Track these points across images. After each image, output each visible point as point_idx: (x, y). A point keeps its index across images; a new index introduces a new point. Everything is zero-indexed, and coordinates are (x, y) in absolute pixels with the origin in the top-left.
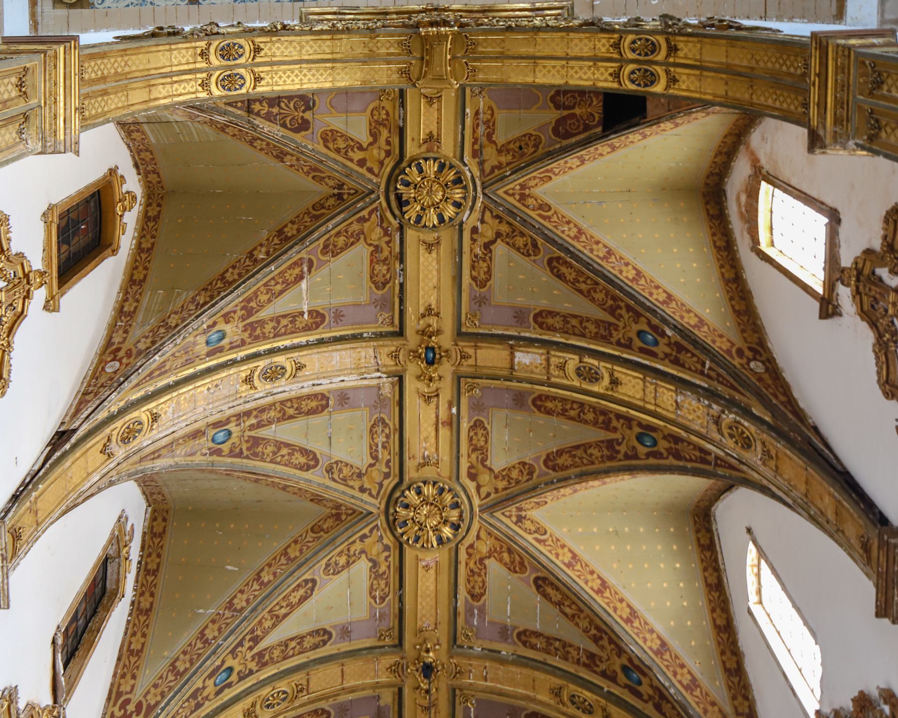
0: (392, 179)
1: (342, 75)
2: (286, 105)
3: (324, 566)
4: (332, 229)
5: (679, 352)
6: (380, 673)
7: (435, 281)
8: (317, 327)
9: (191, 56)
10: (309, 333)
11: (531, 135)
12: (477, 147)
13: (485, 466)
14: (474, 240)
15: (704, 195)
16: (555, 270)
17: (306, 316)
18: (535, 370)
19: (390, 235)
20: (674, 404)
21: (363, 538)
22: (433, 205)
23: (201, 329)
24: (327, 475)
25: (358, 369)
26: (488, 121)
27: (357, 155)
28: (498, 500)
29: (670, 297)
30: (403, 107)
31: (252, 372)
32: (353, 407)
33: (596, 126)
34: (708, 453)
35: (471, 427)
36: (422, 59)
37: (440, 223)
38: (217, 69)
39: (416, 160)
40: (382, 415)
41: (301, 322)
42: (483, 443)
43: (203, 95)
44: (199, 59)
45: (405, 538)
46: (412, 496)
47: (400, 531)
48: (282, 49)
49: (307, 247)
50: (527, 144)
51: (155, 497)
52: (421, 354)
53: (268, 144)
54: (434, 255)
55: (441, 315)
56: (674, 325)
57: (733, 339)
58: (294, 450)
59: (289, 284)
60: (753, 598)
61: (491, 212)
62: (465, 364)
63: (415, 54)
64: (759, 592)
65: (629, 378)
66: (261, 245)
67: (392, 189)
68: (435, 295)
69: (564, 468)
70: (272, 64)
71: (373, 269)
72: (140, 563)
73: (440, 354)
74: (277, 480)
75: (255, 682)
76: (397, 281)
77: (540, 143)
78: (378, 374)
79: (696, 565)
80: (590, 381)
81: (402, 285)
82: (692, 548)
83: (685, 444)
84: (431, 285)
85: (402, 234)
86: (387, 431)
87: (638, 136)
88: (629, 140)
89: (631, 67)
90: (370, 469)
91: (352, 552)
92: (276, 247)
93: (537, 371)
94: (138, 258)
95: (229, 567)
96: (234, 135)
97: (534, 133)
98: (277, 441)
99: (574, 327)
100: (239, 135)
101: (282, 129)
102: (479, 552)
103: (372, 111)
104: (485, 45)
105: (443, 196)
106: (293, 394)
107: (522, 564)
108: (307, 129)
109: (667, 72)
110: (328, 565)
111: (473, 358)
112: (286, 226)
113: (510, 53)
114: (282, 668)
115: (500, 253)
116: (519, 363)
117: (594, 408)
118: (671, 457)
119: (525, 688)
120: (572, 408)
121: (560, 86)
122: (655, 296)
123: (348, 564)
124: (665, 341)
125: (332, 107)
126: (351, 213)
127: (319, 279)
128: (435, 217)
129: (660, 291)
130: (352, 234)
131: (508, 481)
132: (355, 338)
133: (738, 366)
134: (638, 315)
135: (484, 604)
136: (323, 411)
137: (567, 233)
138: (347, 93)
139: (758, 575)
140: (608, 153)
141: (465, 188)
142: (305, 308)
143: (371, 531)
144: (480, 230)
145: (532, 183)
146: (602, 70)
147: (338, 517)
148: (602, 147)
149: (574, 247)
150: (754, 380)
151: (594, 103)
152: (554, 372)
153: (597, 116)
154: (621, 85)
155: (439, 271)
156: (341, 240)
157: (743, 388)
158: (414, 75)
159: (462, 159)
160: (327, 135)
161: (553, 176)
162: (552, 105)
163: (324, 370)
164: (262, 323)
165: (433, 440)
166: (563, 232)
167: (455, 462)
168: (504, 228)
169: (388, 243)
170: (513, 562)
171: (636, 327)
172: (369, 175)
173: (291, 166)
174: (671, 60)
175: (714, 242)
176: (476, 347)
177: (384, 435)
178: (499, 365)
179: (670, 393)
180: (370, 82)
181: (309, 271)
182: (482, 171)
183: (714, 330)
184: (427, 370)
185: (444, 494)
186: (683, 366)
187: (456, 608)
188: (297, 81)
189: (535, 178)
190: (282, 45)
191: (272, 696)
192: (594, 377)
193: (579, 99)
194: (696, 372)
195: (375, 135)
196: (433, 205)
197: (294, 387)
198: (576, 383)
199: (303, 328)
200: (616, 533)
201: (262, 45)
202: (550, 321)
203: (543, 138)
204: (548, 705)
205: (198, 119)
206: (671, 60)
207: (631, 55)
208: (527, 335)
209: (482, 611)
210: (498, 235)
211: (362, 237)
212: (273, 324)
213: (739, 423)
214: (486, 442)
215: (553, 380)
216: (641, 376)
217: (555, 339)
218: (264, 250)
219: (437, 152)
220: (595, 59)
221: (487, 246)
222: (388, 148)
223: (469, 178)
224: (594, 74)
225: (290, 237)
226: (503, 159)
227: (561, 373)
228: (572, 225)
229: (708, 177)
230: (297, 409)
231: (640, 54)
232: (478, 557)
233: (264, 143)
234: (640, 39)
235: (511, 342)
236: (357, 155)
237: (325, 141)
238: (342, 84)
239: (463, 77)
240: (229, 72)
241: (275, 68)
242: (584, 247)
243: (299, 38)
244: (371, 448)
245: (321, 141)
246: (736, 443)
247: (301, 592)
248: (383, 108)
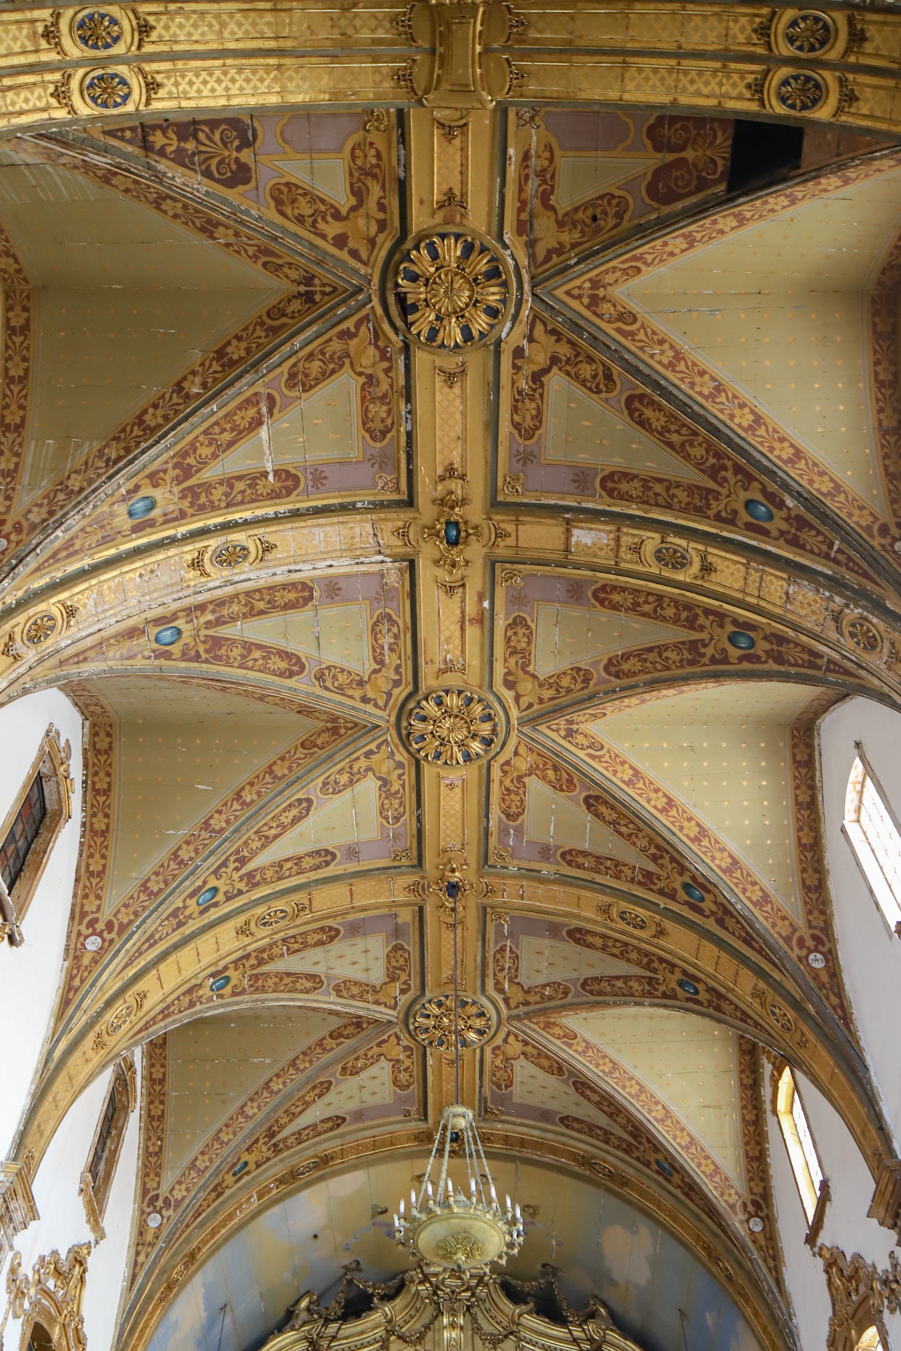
0: (389, 269)
1: (297, 81)
3: (320, 785)
4: (301, 349)
5: (799, 529)
6: (396, 893)
7: (458, 429)
8: (289, 493)
9: (27, 37)
10: (277, 501)
11: (613, 196)
12: (524, 216)
13: (527, 673)
14: (517, 368)
15: (874, 302)
16: (637, 414)
17: (271, 477)
18: (599, 553)
19: (390, 360)
20: (784, 596)
21: (368, 755)
22: (455, 312)
23: (117, 496)
24: (317, 683)
25: (350, 550)
26: (544, 170)
27: (333, 229)
28: (544, 711)
29: (798, 454)
30: (404, 143)
31: (201, 553)
32: (347, 600)
33: (717, 182)
34: (820, 656)
35: (509, 625)
36: (433, 51)
37: (465, 342)
38: (78, 64)
39: (428, 236)
40: (388, 610)
41: (264, 487)
42: (524, 645)
43: (61, 114)
44: (43, 44)
45: (423, 754)
46: (430, 708)
47: (416, 747)
48: (188, 28)
49: (263, 376)
50: (605, 213)
51: (91, 708)
52: (439, 531)
53: (185, 207)
54: (457, 389)
55: (468, 478)
56: (798, 493)
57: (878, 512)
58: (270, 653)
59: (240, 432)
60: (849, 815)
61: (545, 325)
62: (502, 544)
63: (420, 42)
64: (858, 810)
65: (727, 563)
66: (193, 373)
67: (390, 285)
68: (459, 449)
69: (631, 674)
70: (173, 57)
71: (367, 410)
72: (85, 782)
73: (466, 531)
74: (250, 689)
75: (246, 901)
76: (402, 429)
77: (625, 212)
78: (380, 558)
79: (787, 783)
80: (674, 567)
81: (409, 435)
82: (785, 766)
83: (792, 645)
84: (453, 434)
85: (407, 358)
86: (395, 630)
87: (783, 201)
88: (768, 207)
89: (784, 72)
90: (373, 676)
91: (355, 770)
92: (217, 375)
93: (602, 554)
94: (8, 392)
95: (200, 787)
96: (127, 191)
97: (618, 193)
98: (246, 642)
99: (657, 494)
100: (135, 191)
101: (206, 181)
102: (517, 769)
103: (353, 149)
104: (540, 26)
105: (470, 298)
106: (262, 583)
107: (570, 782)
108: (247, 181)
109: (842, 82)
110: (325, 784)
111: (513, 537)
112: (228, 343)
113: (582, 43)
114: (277, 889)
115: (556, 387)
116: (578, 543)
117: (676, 602)
118: (770, 661)
119: (569, 905)
120: (646, 602)
121: (663, 107)
122: (777, 453)
123: (351, 783)
124: (783, 514)
125: (285, 141)
126: (329, 324)
127: (286, 425)
128: (458, 331)
129: (786, 444)
130: (331, 357)
131: (557, 690)
132: (345, 508)
133: (878, 548)
134: (750, 478)
135: (522, 824)
136: (305, 605)
137: (657, 358)
138: (308, 116)
139: (861, 793)
140: (733, 229)
141: (505, 284)
142: (269, 467)
143: (379, 747)
144: (527, 353)
145: (609, 278)
146: (736, 77)
147: (335, 731)
148: (724, 220)
149: (666, 379)
150: (896, 566)
151: (718, 141)
152: (624, 554)
153: (720, 164)
154: (764, 106)
155: (464, 414)
156: (315, 367)
157: (879, 575)
158: (420, 84)
159: (500, 237)
160: (281, 192)
161: (643, 268)
162: (649, 143)
163: (303, 551)
165: (458, 642)
166: (652, 356)
167: (487, 667)
168: (564, 350)
169: (387, 371)
170: (559, 780)
171: (744, 496)
172: (353, 263)
173: (228, 245)
174: (852, 59)
175: (876, 374)
176: (518, 522)
177: (391, 634)
178: (550, 546)
179: (780, 583)
180: (346, 95)
181: (271, 412)
182: (532, 257)
183: (854, 499)
184: (448, 551)
185: (472, 705)
186: (803, 547)
187: (487, 828)
188: (220, 90)
189: (614, 269)
190: (187, 18)
191: (269, 914)
192: (679, 561)
193: (693, 133)
194: (818, 555)
195: (359, 194)
196: (455, 312)
197: (262, 573)
198: (655, 570)
199: (268, 494)
200: (692, 748)
201: (151, 20)
202: (624, 487)
203: (630, 199)
204: (594, 922)
205: (63, 160)
206: (852, 59)
207: (786, 50)
208: (591, 505)
209: (519, 831)
210: (554, 360)
211: (347, 361)
212: (224, 488)
213: (866, 619)
214: (529, 643)
215: (623, 565)
216: (744, 561)
217: (630, 512)
218: (198, 380)
219: (461, 224)
220: (726, 56)
221: (537, 377)
222: (381, 216)
223: (512, 269)
224: (721, 85)
225: (237, 361)
226: (567, 238)
227: (635, 557)
228: (666, 346)
229: (884, 272)
230: (269, 602)
231: (800, 48)
232: (515, 775)
233: (179, 205)
234: (804, 18)
235: (567, 516)
236: (333, 229)
237: (279, 202)
238: (298, 98)
239: (504, 86)
240: (99, 72)
241: (180, 65)
242: (682, 380)
243: (215, 6)
244: (374, 650)
245: (272, 204)
246: (858, 643)
247: (294, 812)
248: (371, 144)
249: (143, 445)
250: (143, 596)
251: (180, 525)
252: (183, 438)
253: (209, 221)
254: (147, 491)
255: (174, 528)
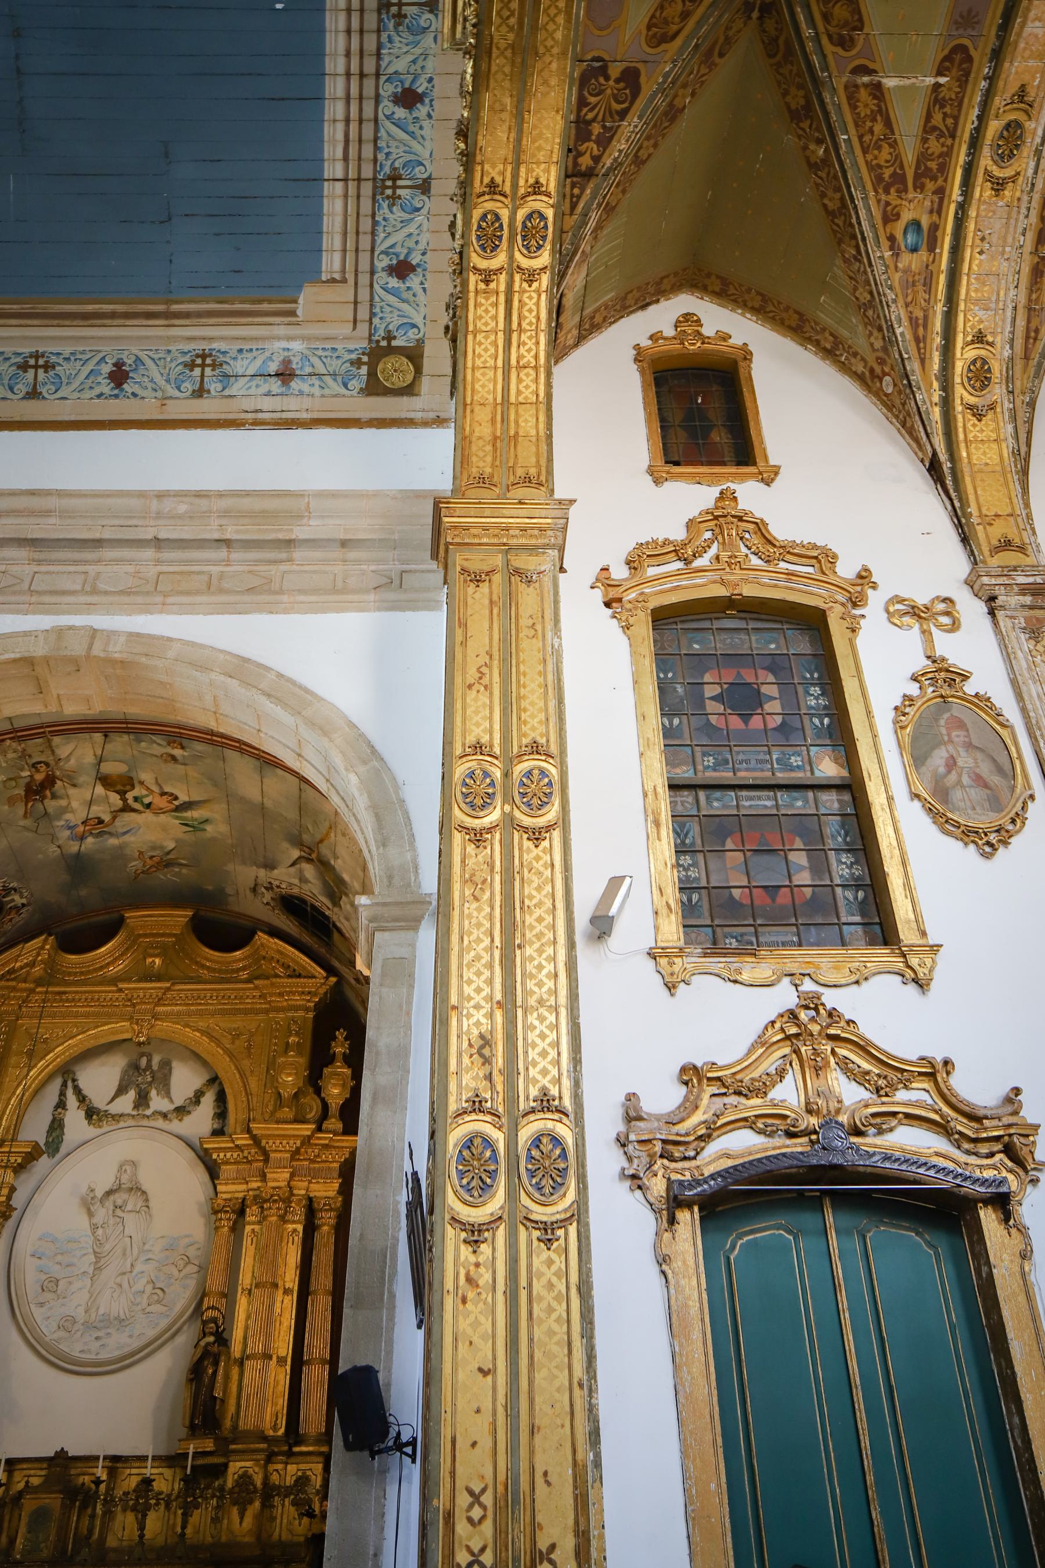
2: (591, 110)
53: (648, 138)
66: (805, 148)
101: (628, 117)
164: (923, 158)
233: (646, 143)
249: (854, 220)
250: (1003, 253)
251: (950, 196)
252: (861, 178)
253: (666, 114)
254: (898, 228)
255: (949, 203)
